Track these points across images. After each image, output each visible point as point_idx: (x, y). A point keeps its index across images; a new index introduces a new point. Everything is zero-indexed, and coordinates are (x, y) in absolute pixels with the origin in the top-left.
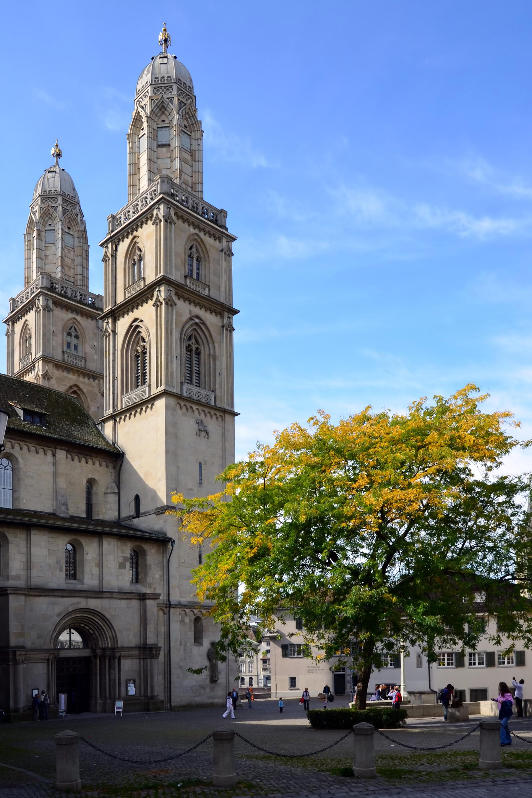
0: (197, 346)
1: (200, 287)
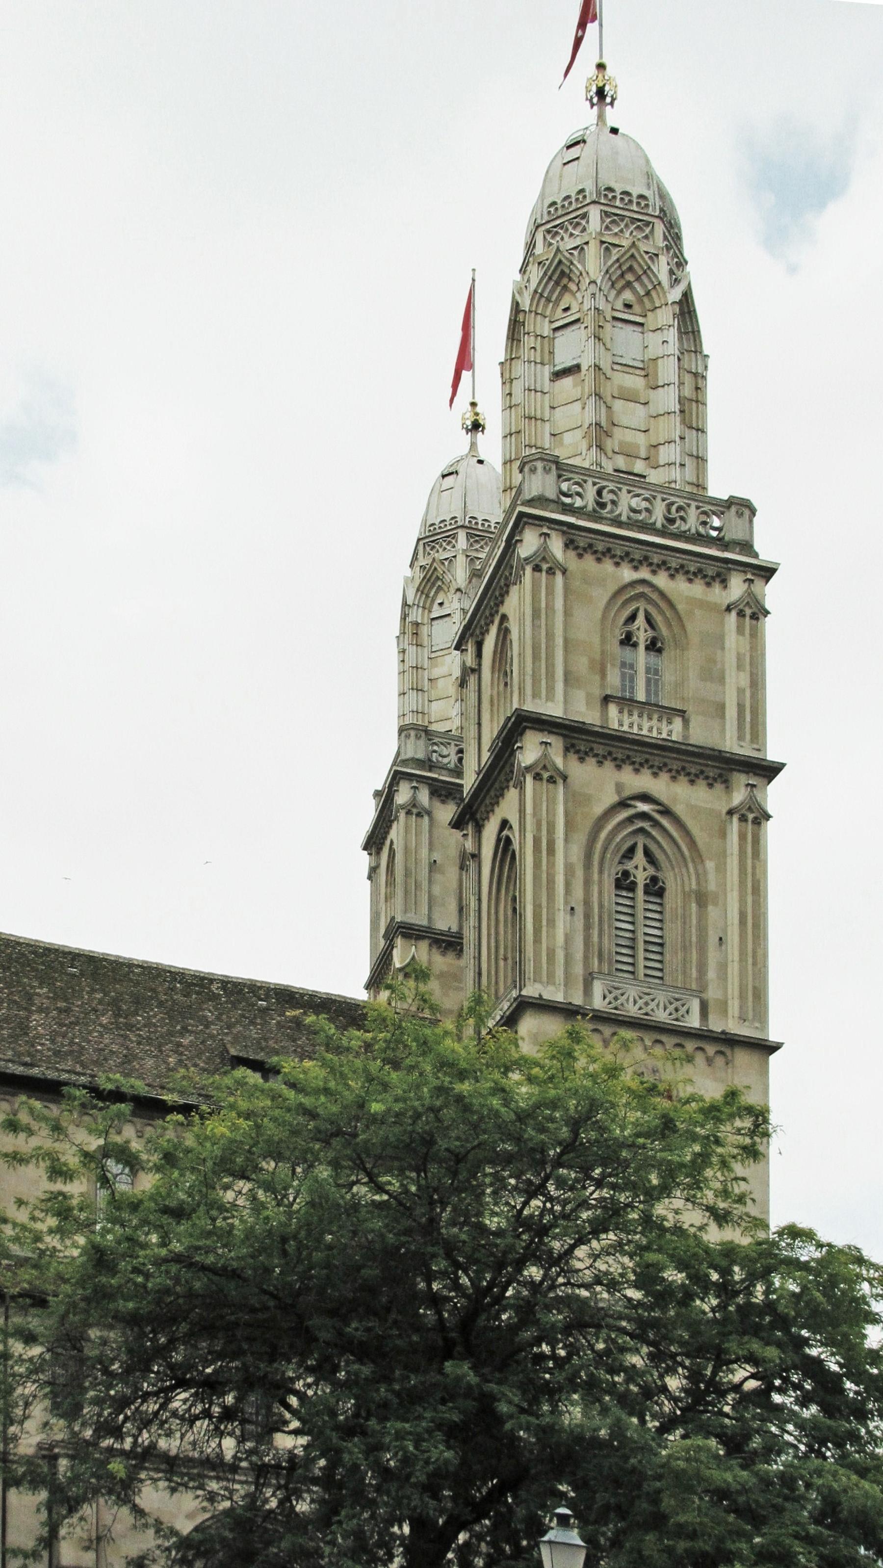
0: (651, 871)
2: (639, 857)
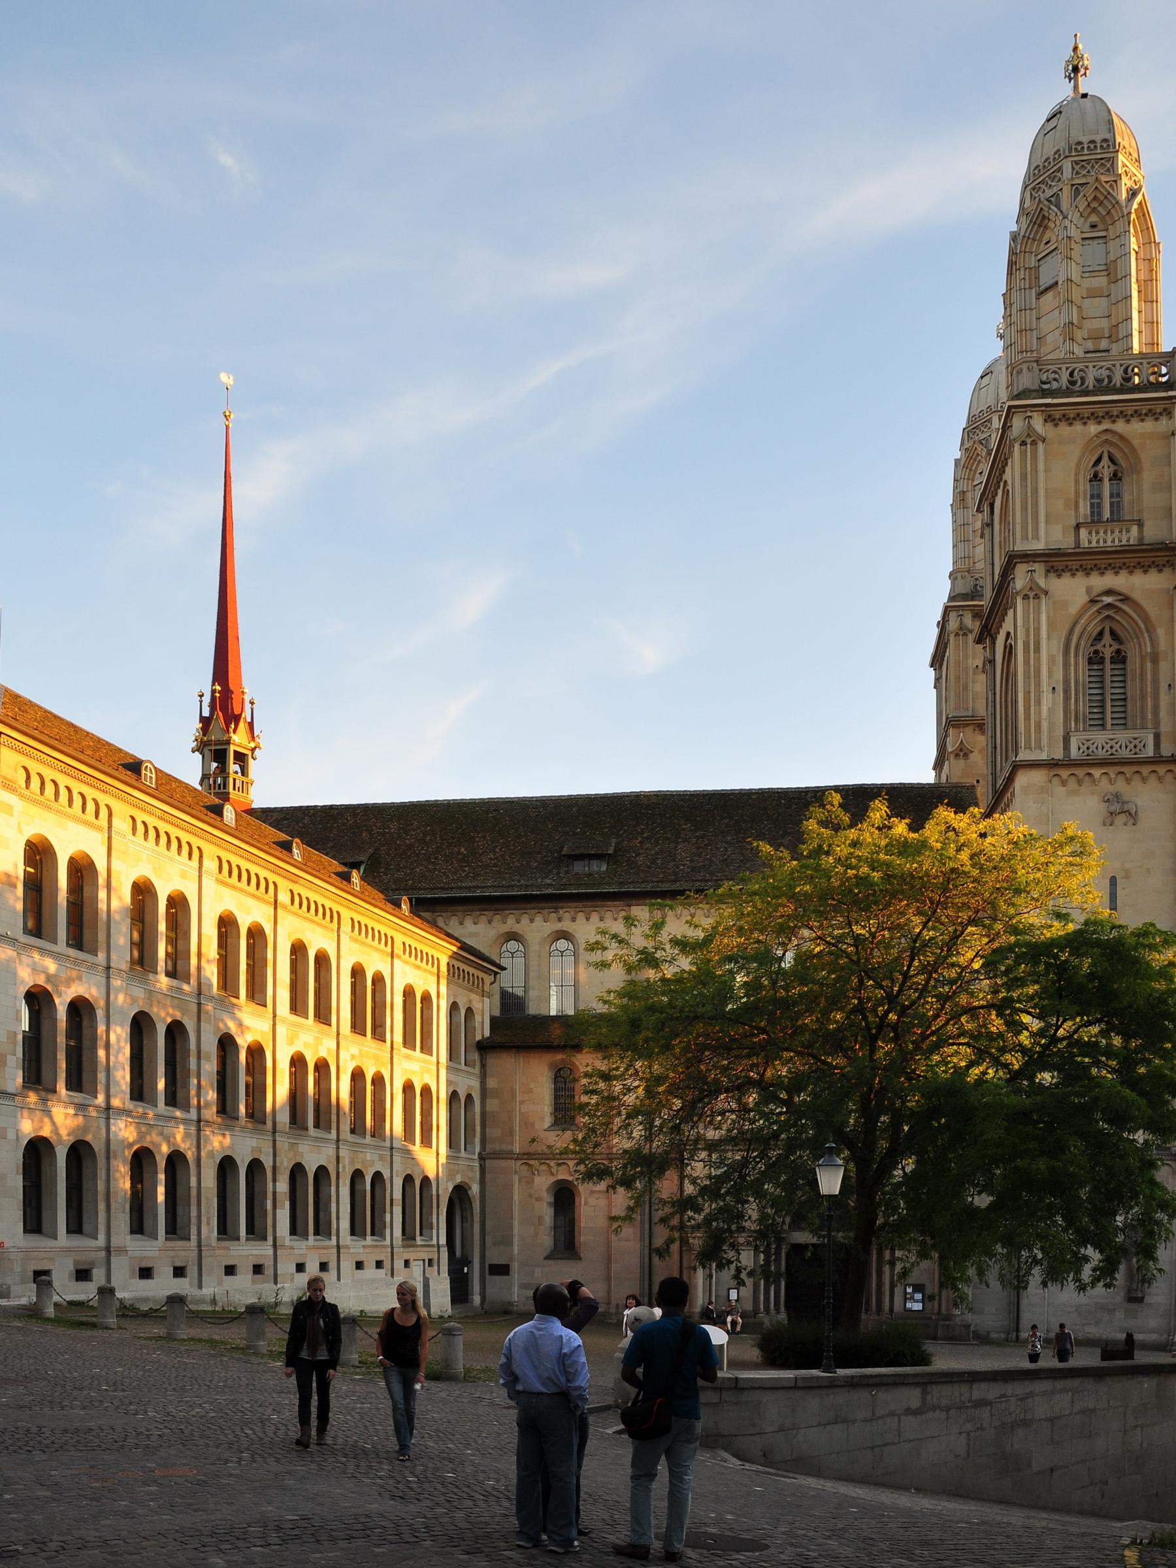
0: (1116, 646)
1: (1102, 532)
2: (1107, 639)
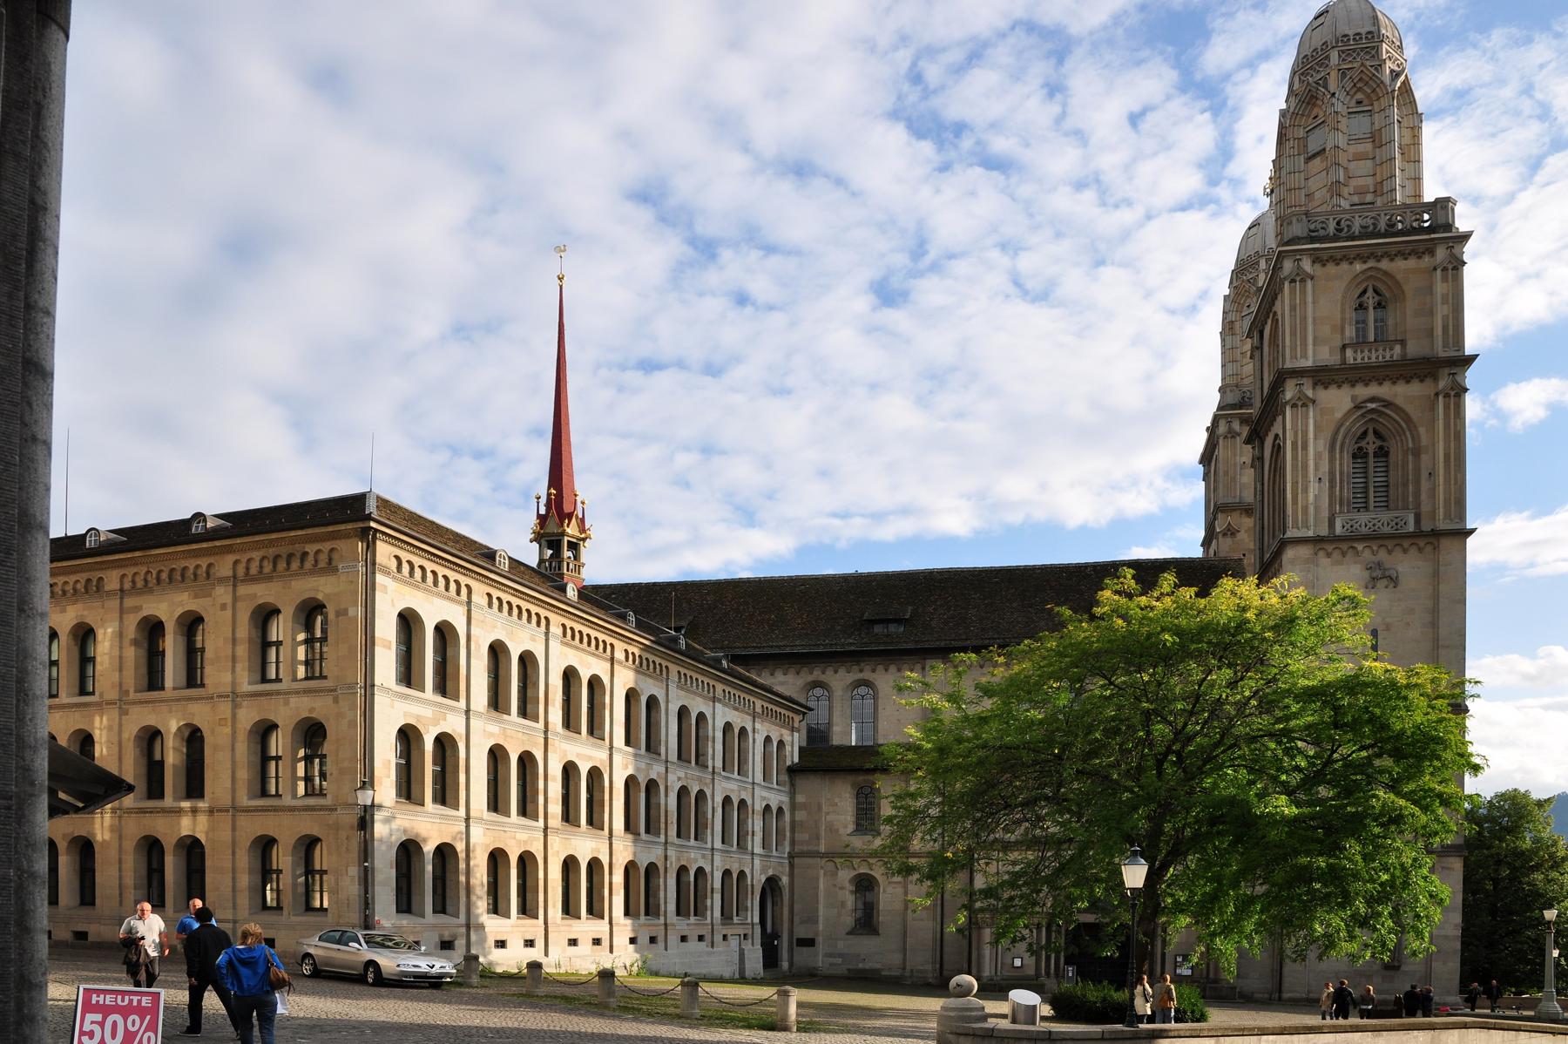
0: (1379, 443)
2: (1371, 437)
